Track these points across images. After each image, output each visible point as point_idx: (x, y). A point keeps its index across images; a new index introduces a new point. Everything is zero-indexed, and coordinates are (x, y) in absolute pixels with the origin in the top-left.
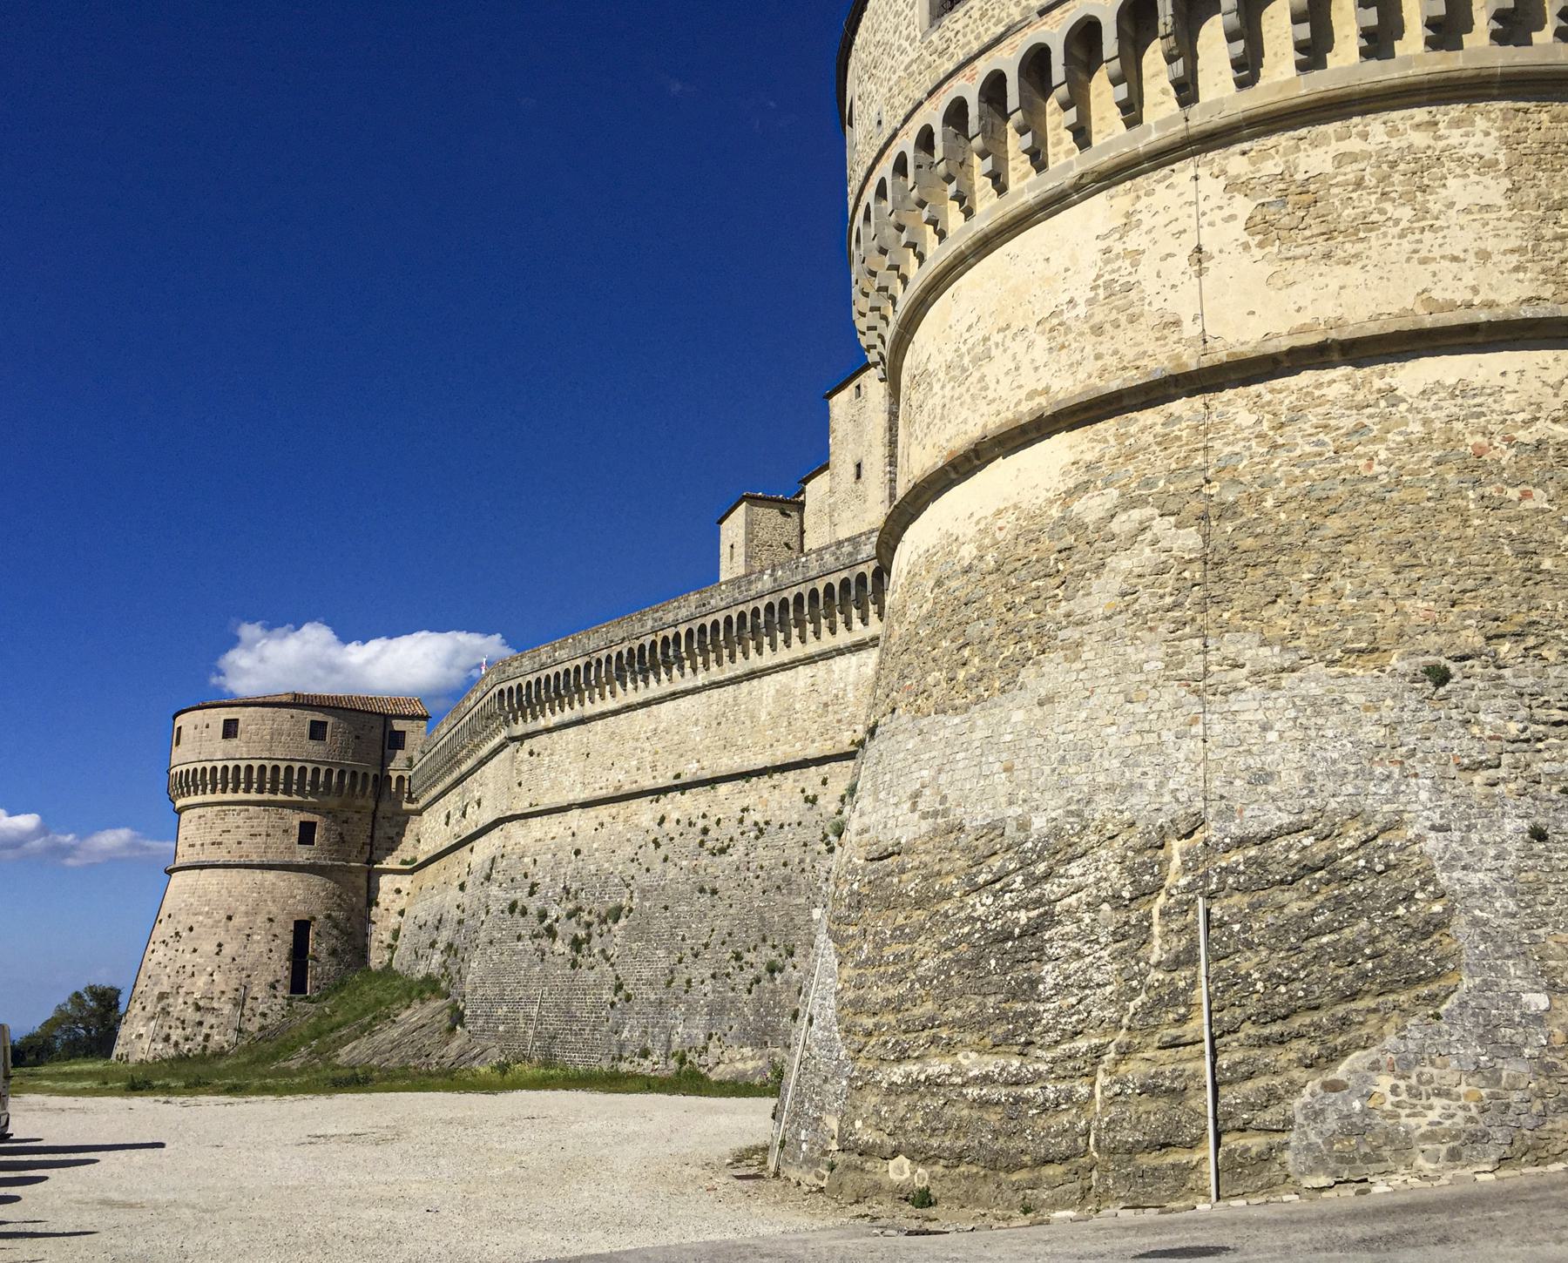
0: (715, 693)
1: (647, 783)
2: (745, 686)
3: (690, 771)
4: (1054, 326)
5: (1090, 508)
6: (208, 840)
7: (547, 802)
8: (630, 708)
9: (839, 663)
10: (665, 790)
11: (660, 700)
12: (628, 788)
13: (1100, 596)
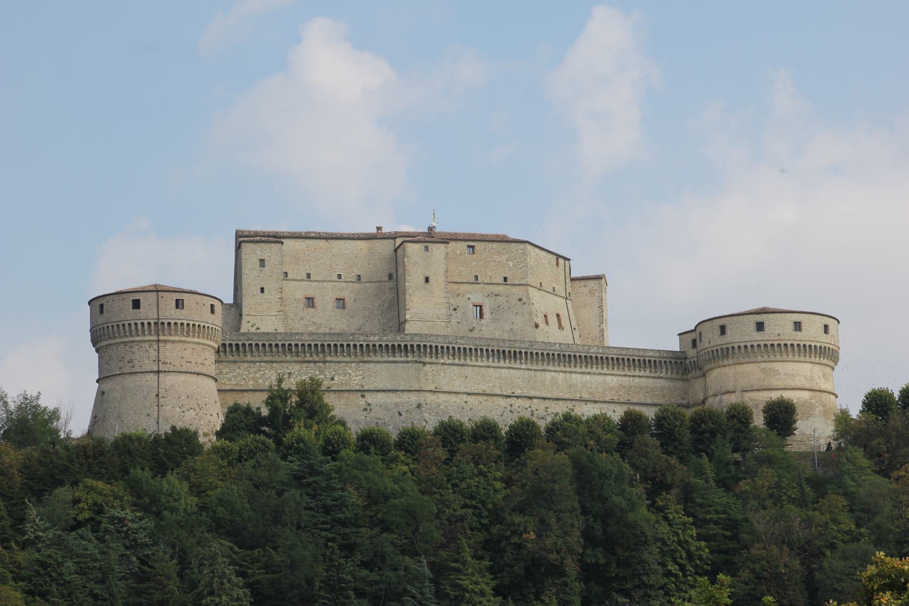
0: (526, 372)
1: (498, 392)
2: (539, 373)
3: (518, 392)
4: (805, 377)
5: (813, 401)
6: (199, 361)
7: (445, 389)
8: (488, 367)
9: (574, 376)
10: (509, 397)
11: (502, 368)
12: (488, 392)
13: (816, 412)
